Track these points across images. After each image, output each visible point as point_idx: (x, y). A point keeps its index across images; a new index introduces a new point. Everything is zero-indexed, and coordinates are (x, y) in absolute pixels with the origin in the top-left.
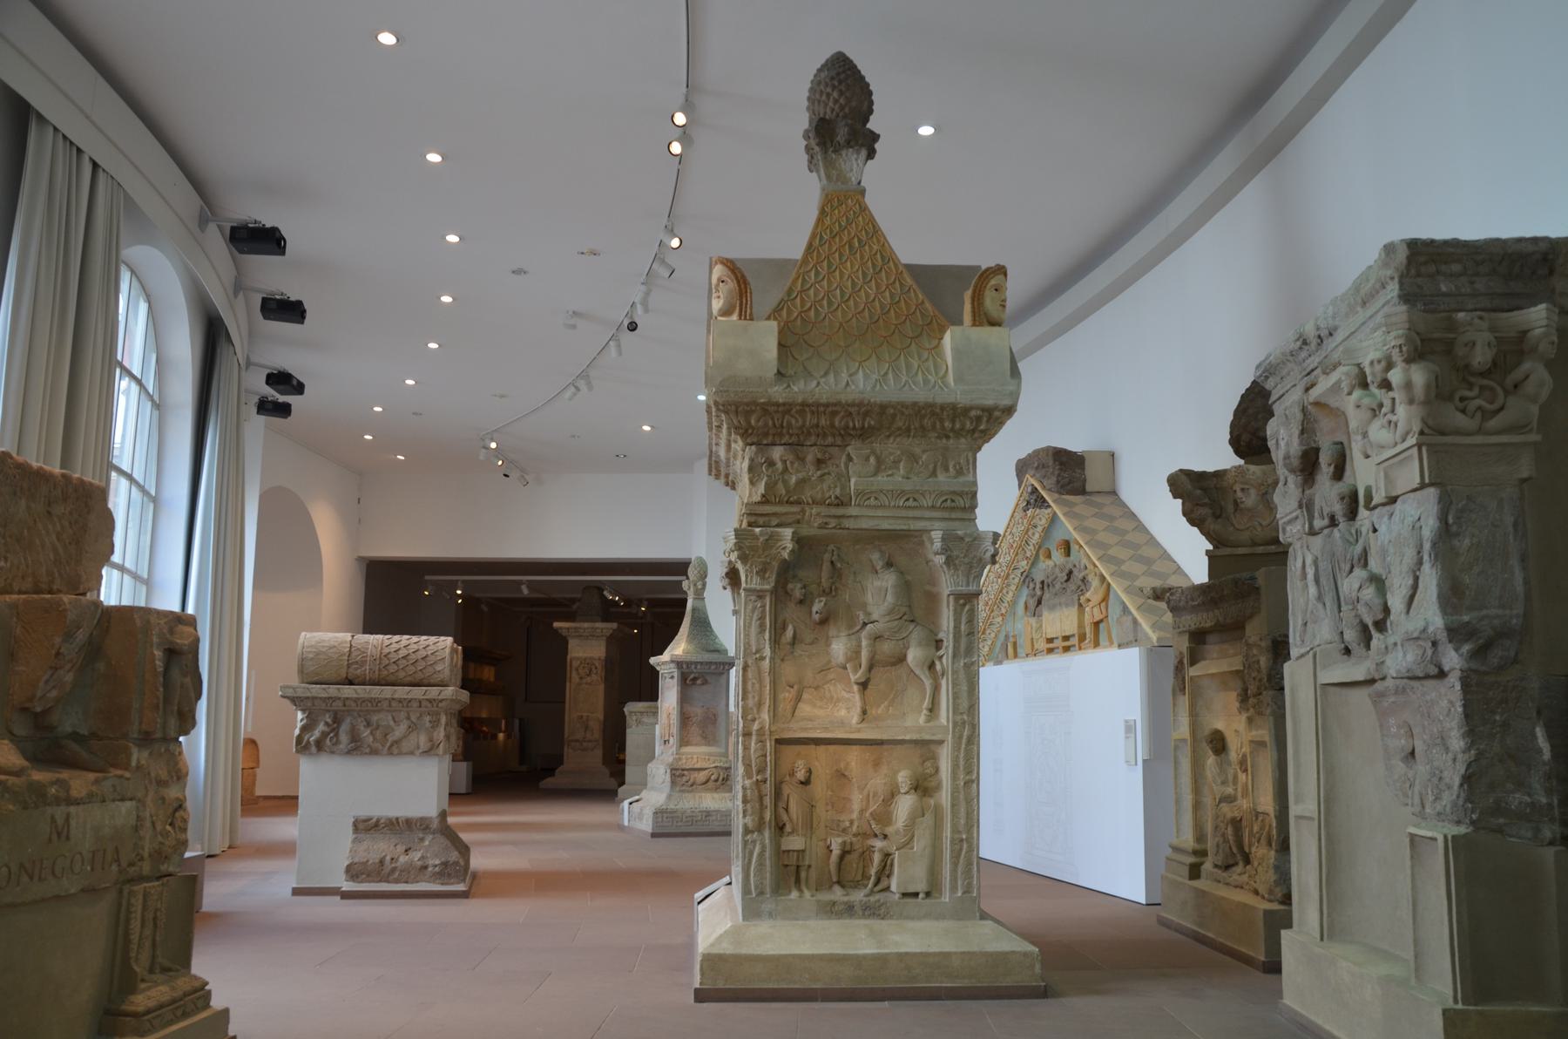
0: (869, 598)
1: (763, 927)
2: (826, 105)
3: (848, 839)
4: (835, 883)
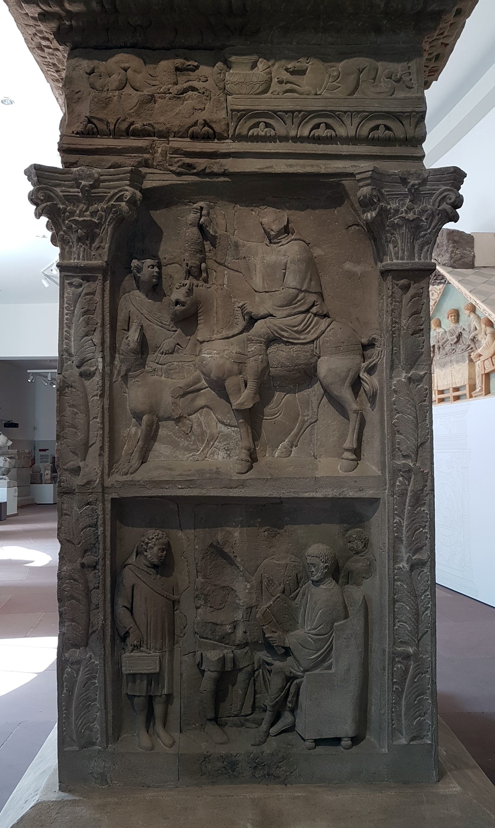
3: (228, 652)
4: (210, 720)
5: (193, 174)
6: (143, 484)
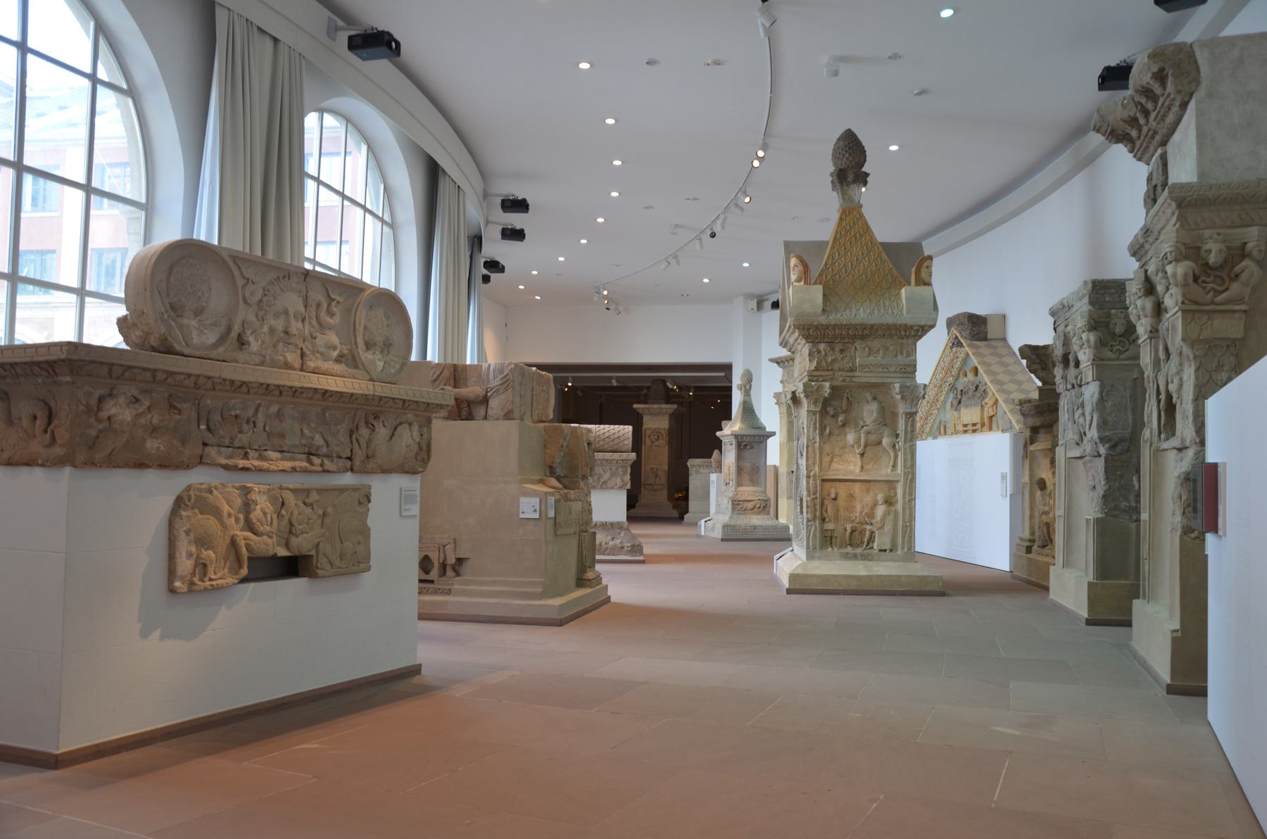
0: (865, 414)
1: (816, 563)
2: (842, 160)
3: (855, 525)
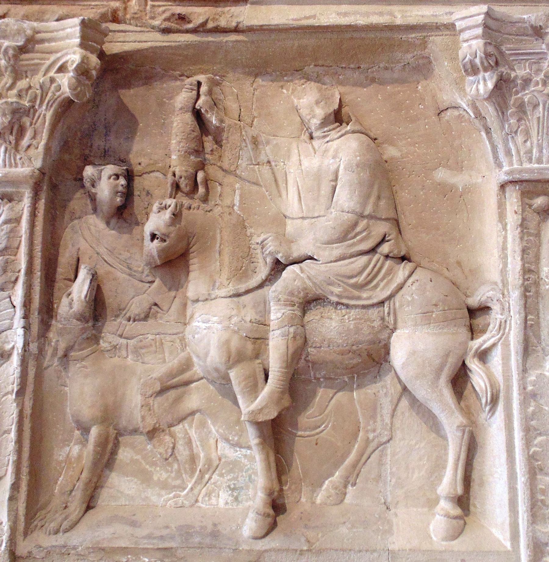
5: (187, 31)
6: (82, 553)
